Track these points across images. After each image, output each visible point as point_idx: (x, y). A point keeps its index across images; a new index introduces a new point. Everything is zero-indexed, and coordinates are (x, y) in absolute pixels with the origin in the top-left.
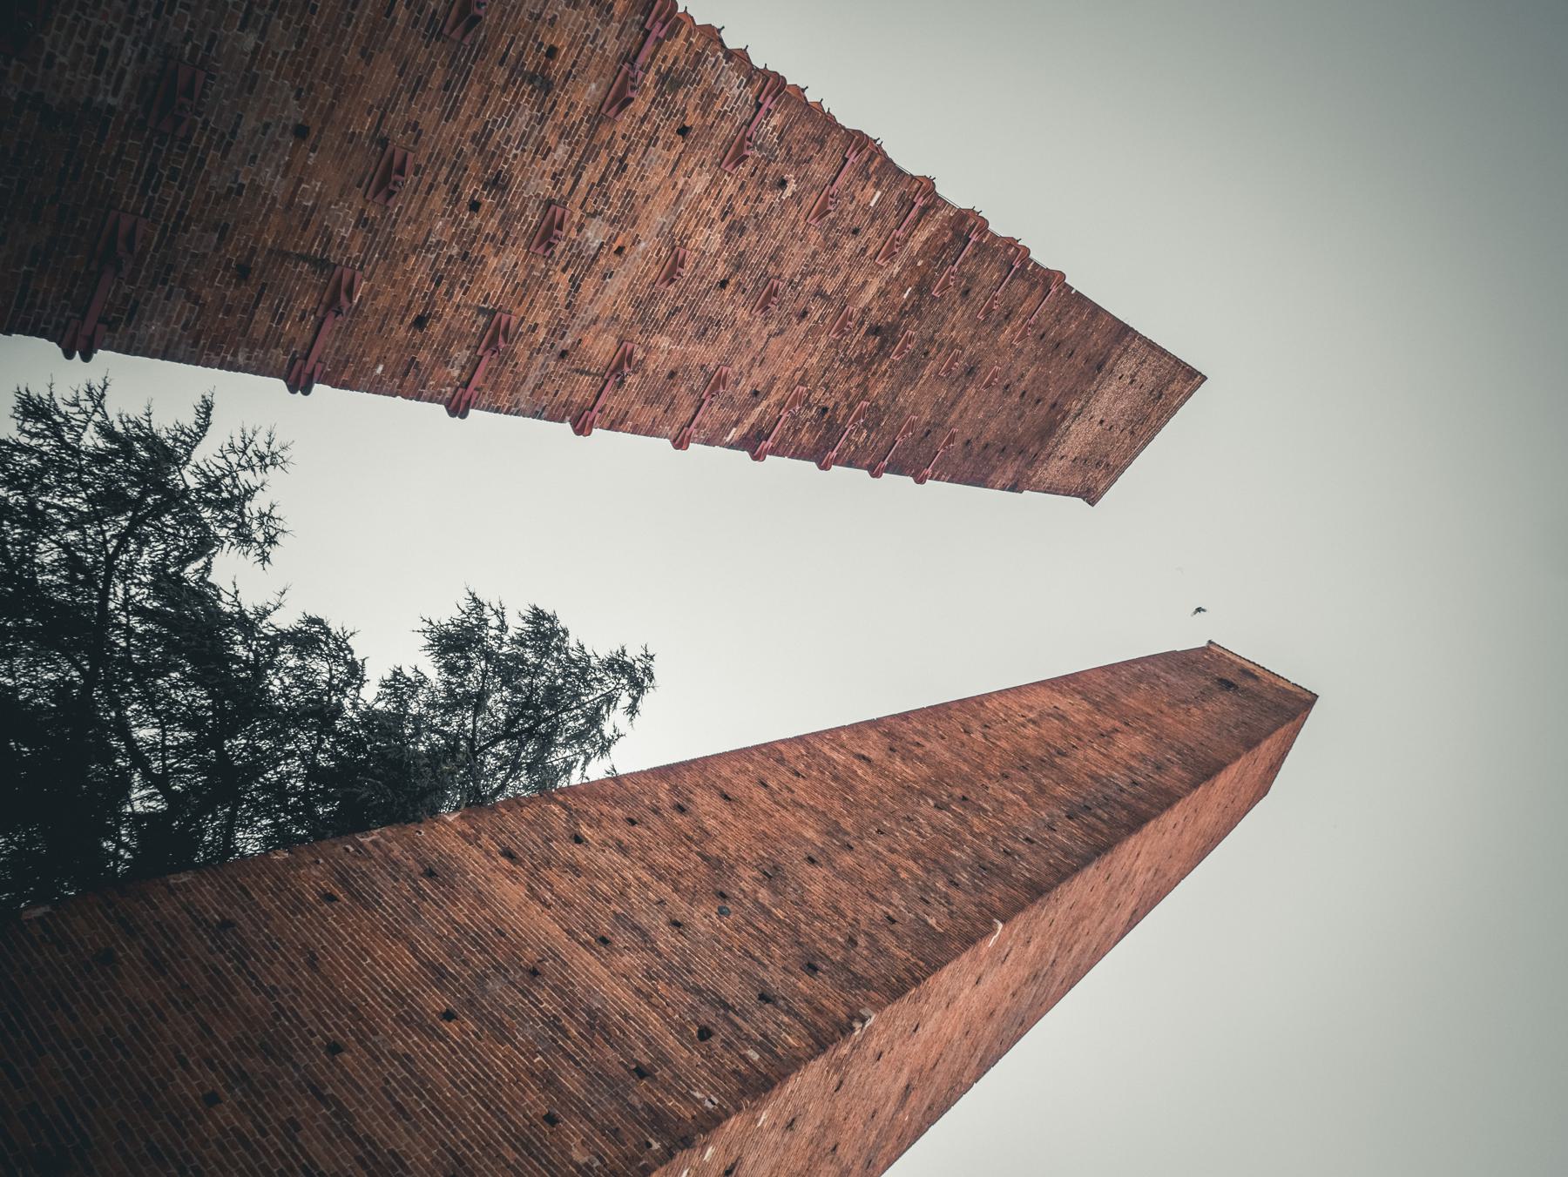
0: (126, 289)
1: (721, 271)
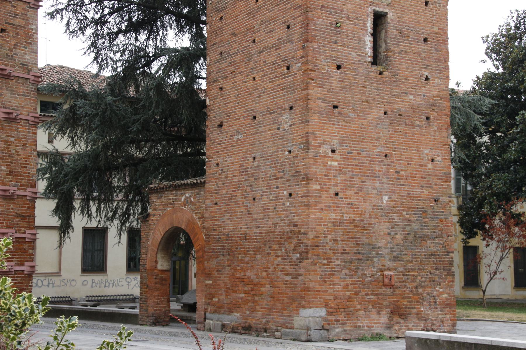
0: (17, 68)
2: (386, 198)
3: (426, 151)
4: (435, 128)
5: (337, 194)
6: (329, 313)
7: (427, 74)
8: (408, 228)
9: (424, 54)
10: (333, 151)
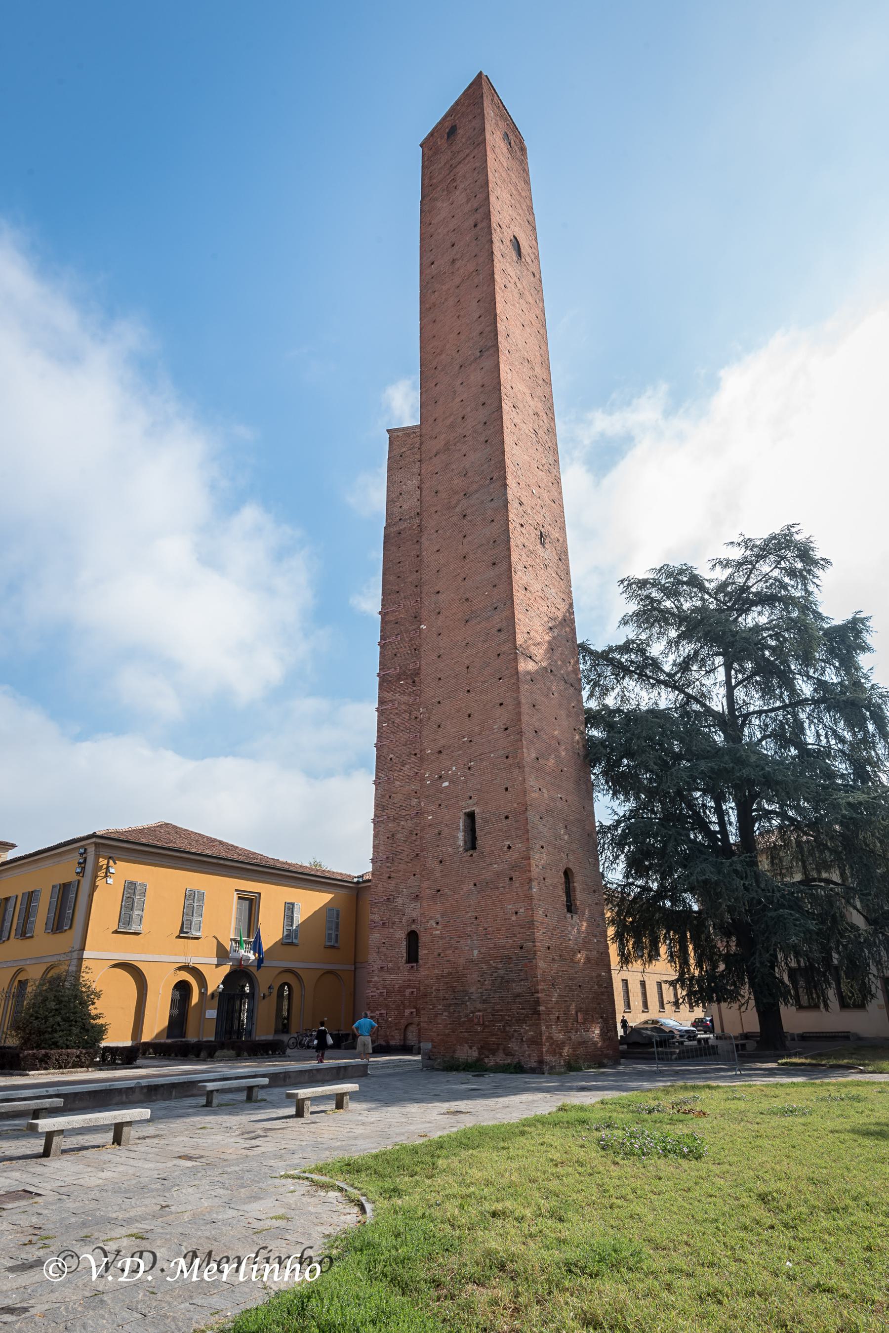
1: (413, 758)
2: (476, 952)
3: (510, 907)
4: (518, 885)
5: (439, 955)
6: (434, 1047)
7: (508, 843)
8: (495, 975)
9: (505, 829)
10: (437, 923)
